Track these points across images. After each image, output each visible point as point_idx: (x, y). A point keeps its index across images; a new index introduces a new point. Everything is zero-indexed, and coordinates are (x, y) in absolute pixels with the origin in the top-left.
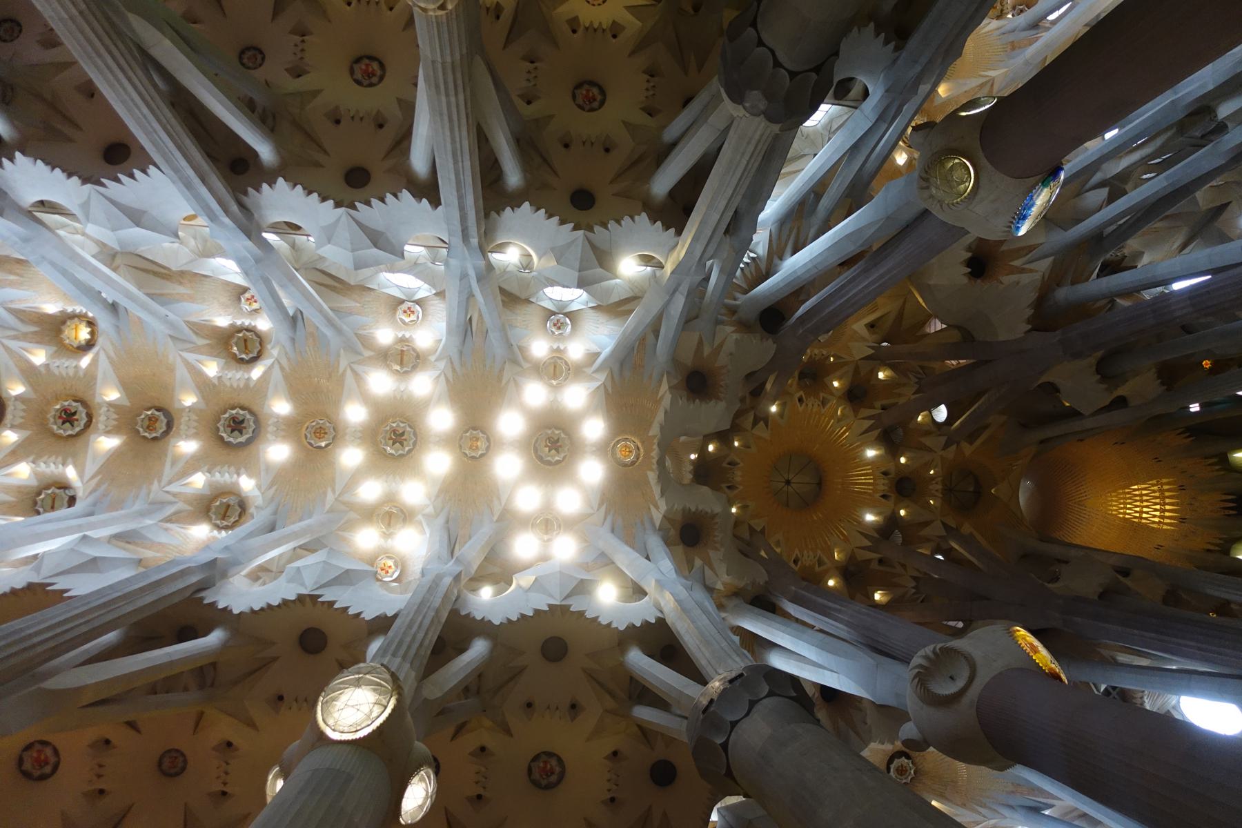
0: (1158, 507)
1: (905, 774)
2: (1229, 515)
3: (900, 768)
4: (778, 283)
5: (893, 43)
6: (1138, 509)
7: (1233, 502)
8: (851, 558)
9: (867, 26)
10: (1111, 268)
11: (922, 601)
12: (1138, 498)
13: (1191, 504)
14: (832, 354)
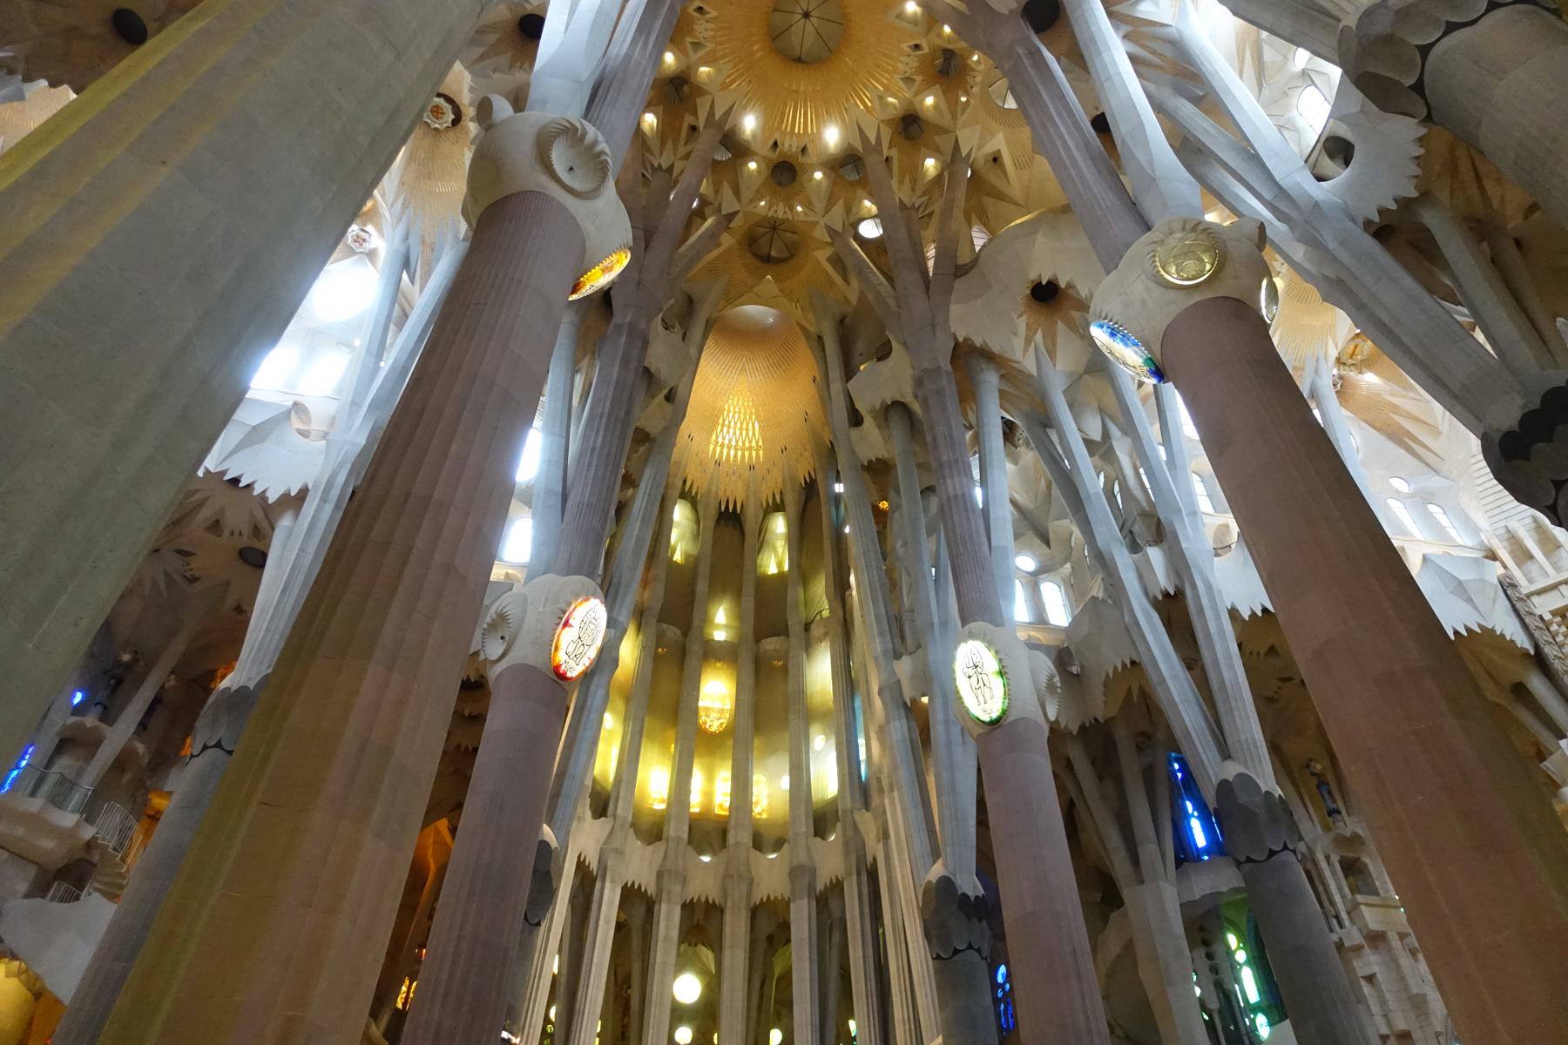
0: (733, 443)
1: (434, 116)
2: (720, 504)
3: (440, 111)
4: (1098, 23)
5: (1376, 219)
6: (732, 424)
7: (733, 510)
8: (699, 90)
9: (1415, 188)
10: (1009, 429)
11: (643, 175)
12: (744, 426)
13: (734, 473)
14: (971, 101)
